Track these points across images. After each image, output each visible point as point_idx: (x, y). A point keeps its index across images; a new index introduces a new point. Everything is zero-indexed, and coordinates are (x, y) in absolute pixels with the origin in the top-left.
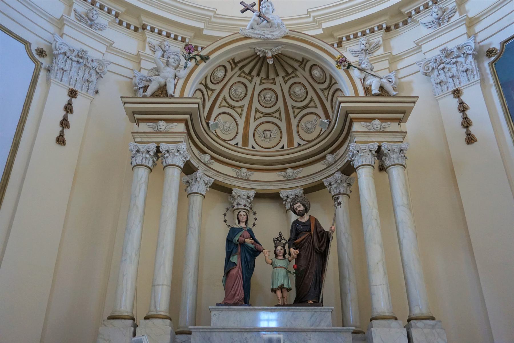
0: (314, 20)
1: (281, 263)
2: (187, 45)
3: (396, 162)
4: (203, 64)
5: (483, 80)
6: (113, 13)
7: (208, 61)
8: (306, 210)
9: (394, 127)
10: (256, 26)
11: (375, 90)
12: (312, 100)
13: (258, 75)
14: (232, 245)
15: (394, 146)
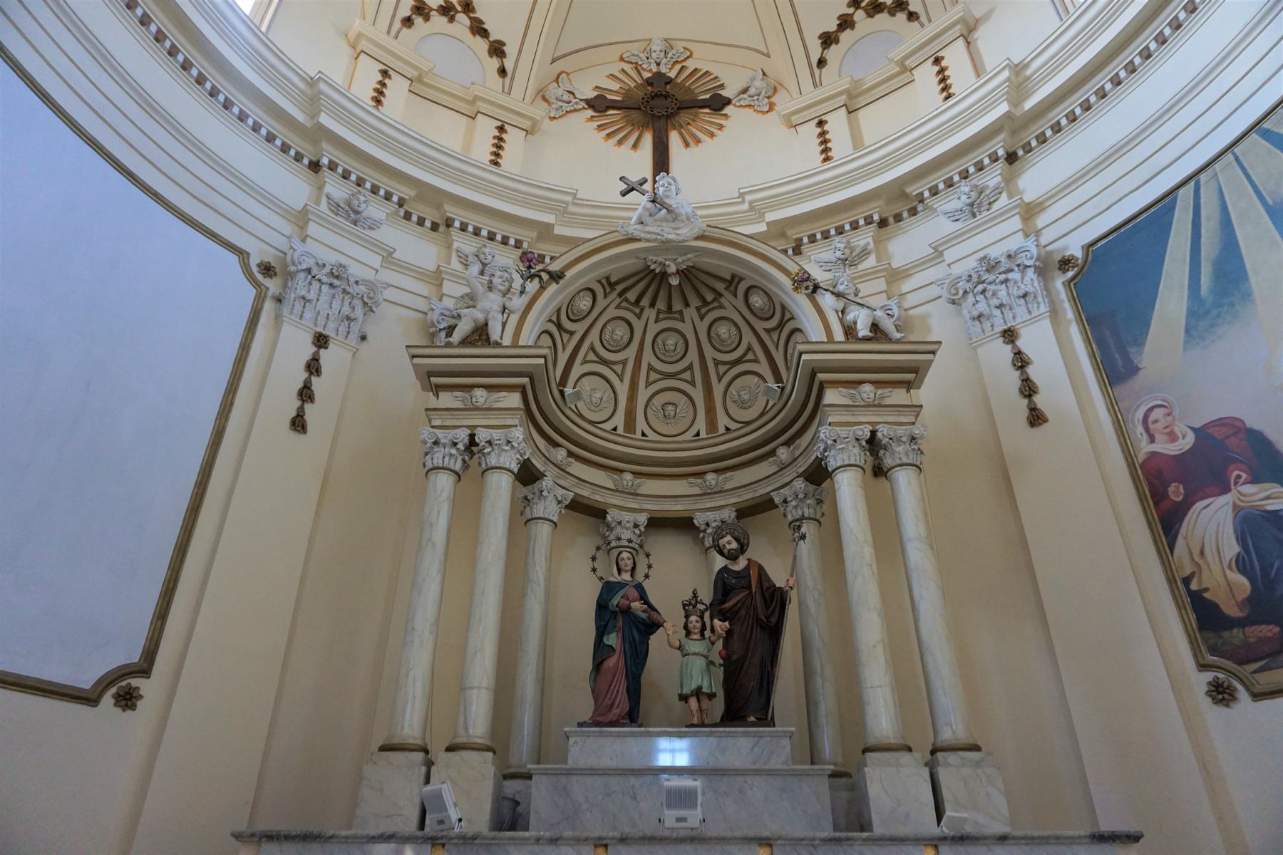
0: (752, 208)
1: (695, 646)
2: (524, 253)
3: (905, 460)
4: (553, 287)
5: (1054, 313)
6: (395, 199)
7: (562, 282)
8: (743, 549)
9: (898, 396)
10: (647, 219)
11: (863, 331)
12: (749, 349)
13: (652, 305)
14: (606, 614)
15: (901, 431)
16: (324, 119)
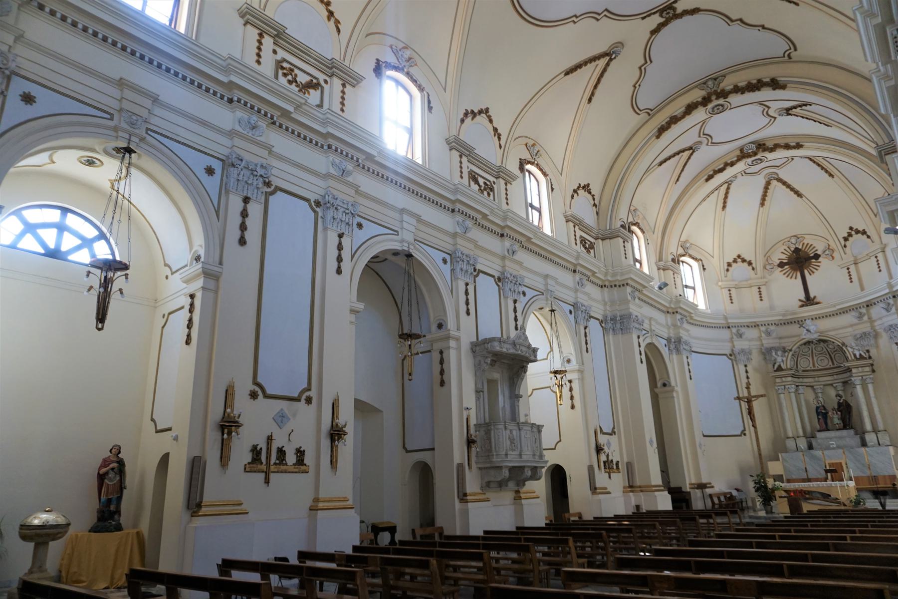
16: (729, 321)
